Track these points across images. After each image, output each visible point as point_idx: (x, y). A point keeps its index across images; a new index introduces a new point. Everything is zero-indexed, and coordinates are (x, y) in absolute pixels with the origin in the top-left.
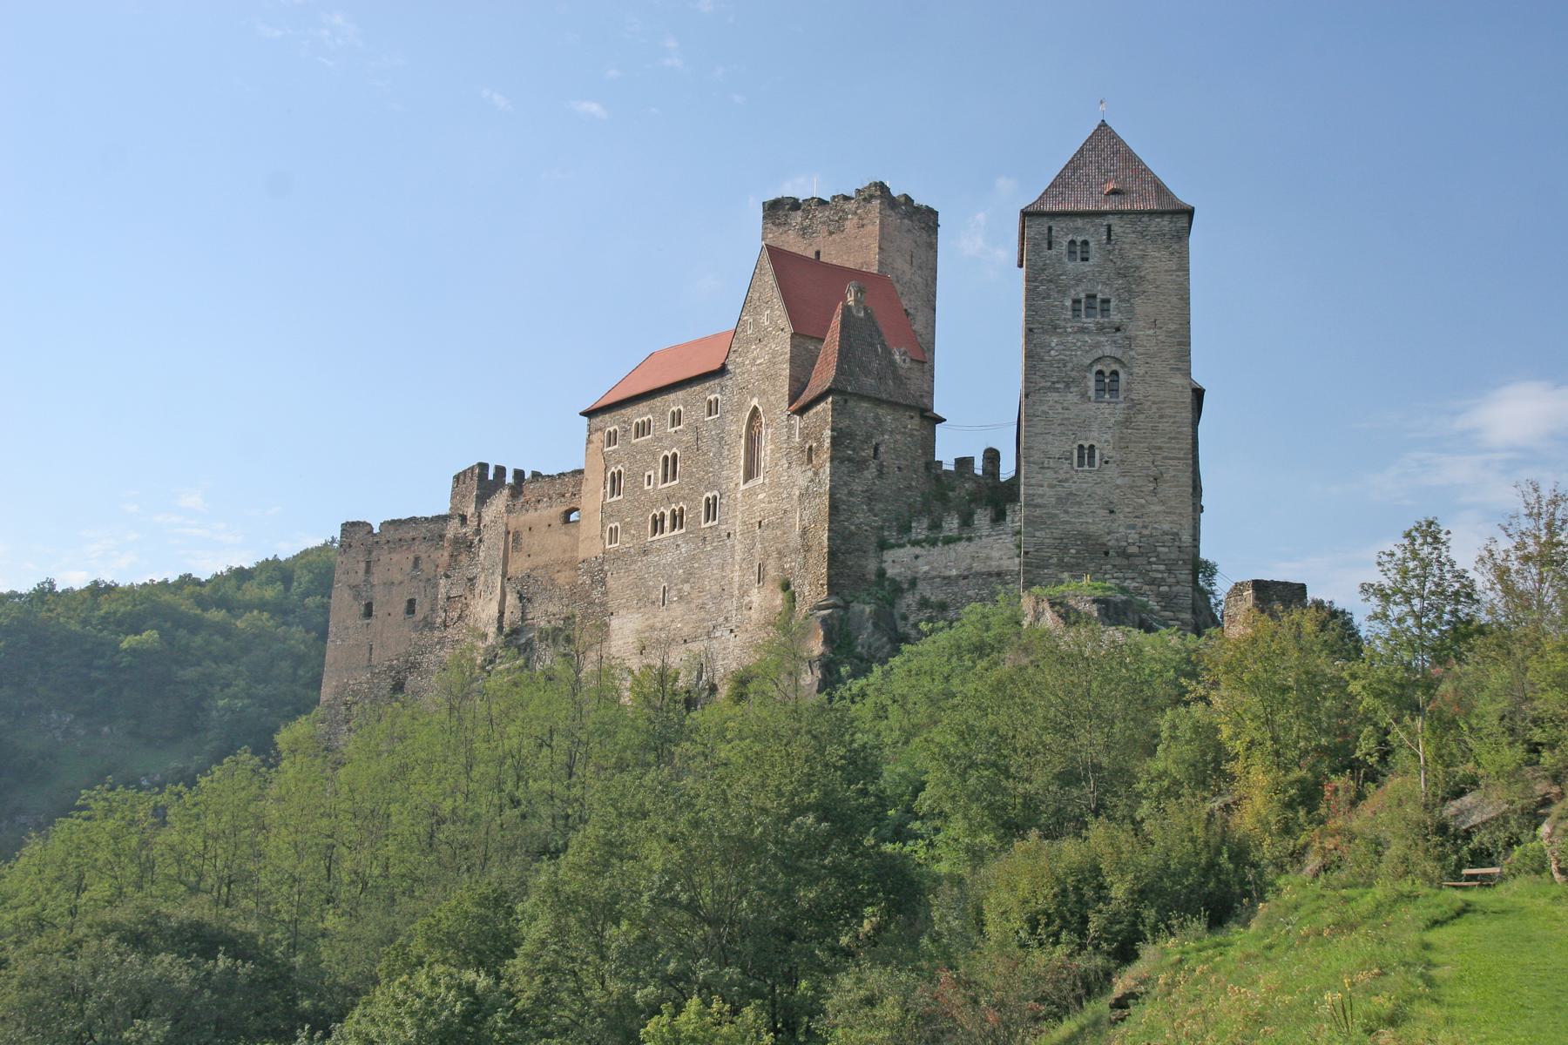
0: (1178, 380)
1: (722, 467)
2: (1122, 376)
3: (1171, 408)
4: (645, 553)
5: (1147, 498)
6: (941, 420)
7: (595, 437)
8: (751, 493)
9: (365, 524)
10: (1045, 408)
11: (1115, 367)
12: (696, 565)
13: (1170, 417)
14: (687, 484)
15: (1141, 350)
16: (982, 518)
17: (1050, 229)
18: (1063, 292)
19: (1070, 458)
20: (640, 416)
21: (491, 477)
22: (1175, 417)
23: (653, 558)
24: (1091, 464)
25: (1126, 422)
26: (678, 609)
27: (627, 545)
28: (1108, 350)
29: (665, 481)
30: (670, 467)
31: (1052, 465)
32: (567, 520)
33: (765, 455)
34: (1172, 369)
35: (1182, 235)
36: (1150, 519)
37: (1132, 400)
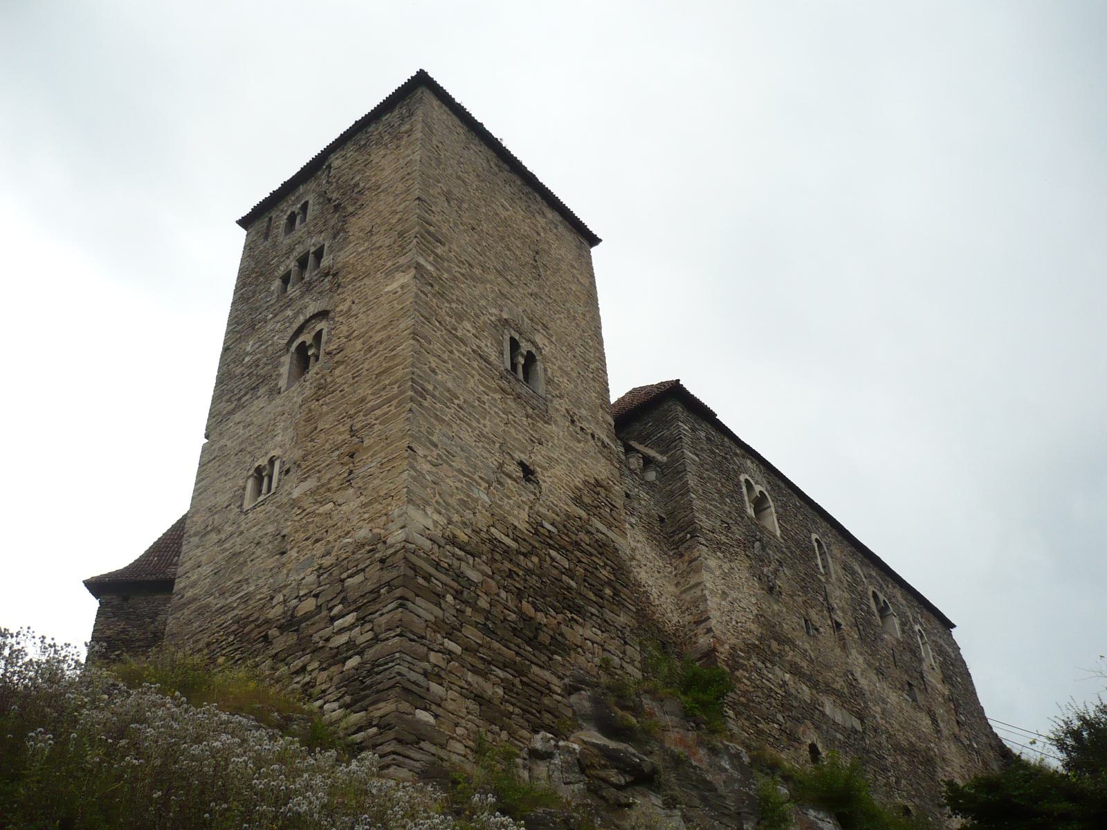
28: (312, 309)
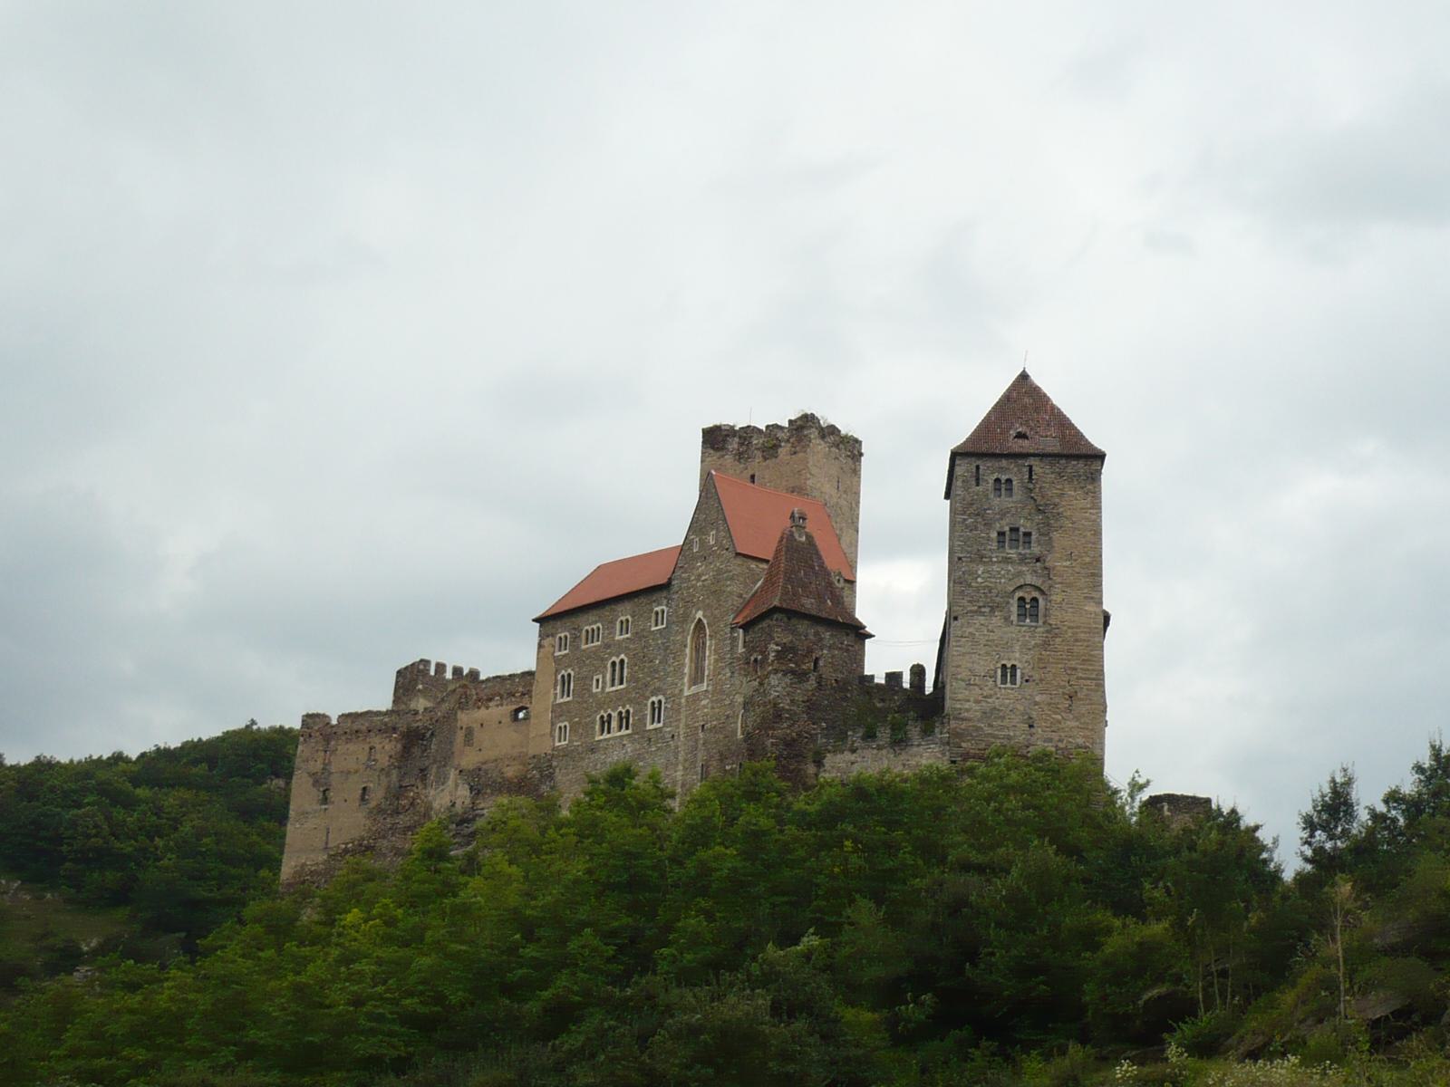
0: (1090, 607)
1: (667, 675)
2: (1041, 601)
3: (1085, 633)
4: (593, 751)
5: (1063, 714)
6: (870, 636)
7: (546, 643)
8: (695, 698)
9: (324, 716)
10: (971, 630)
11: (1036, 594)
12: (641, 764)
13: (1084, 640)
14: (634, 688)
15: (1059, 580)
16: (914, 731)
17: (978, 467)
18: (988, 525)
19: (994, 676)
20: (590, 624)
21: (432, 673)
22: (1089, 641)
23: (596, 756)
24: (1013, 682)
25: (1046, 645)
27: (575, 744)
28: (1029, 579)
29: (613, 685)
31: (977, 682)
32: (516, 719)
33: (709, 664)
34: (1085, 598)
35: (1095, 477)
36: (1066, 734)
37: (1051, 625)
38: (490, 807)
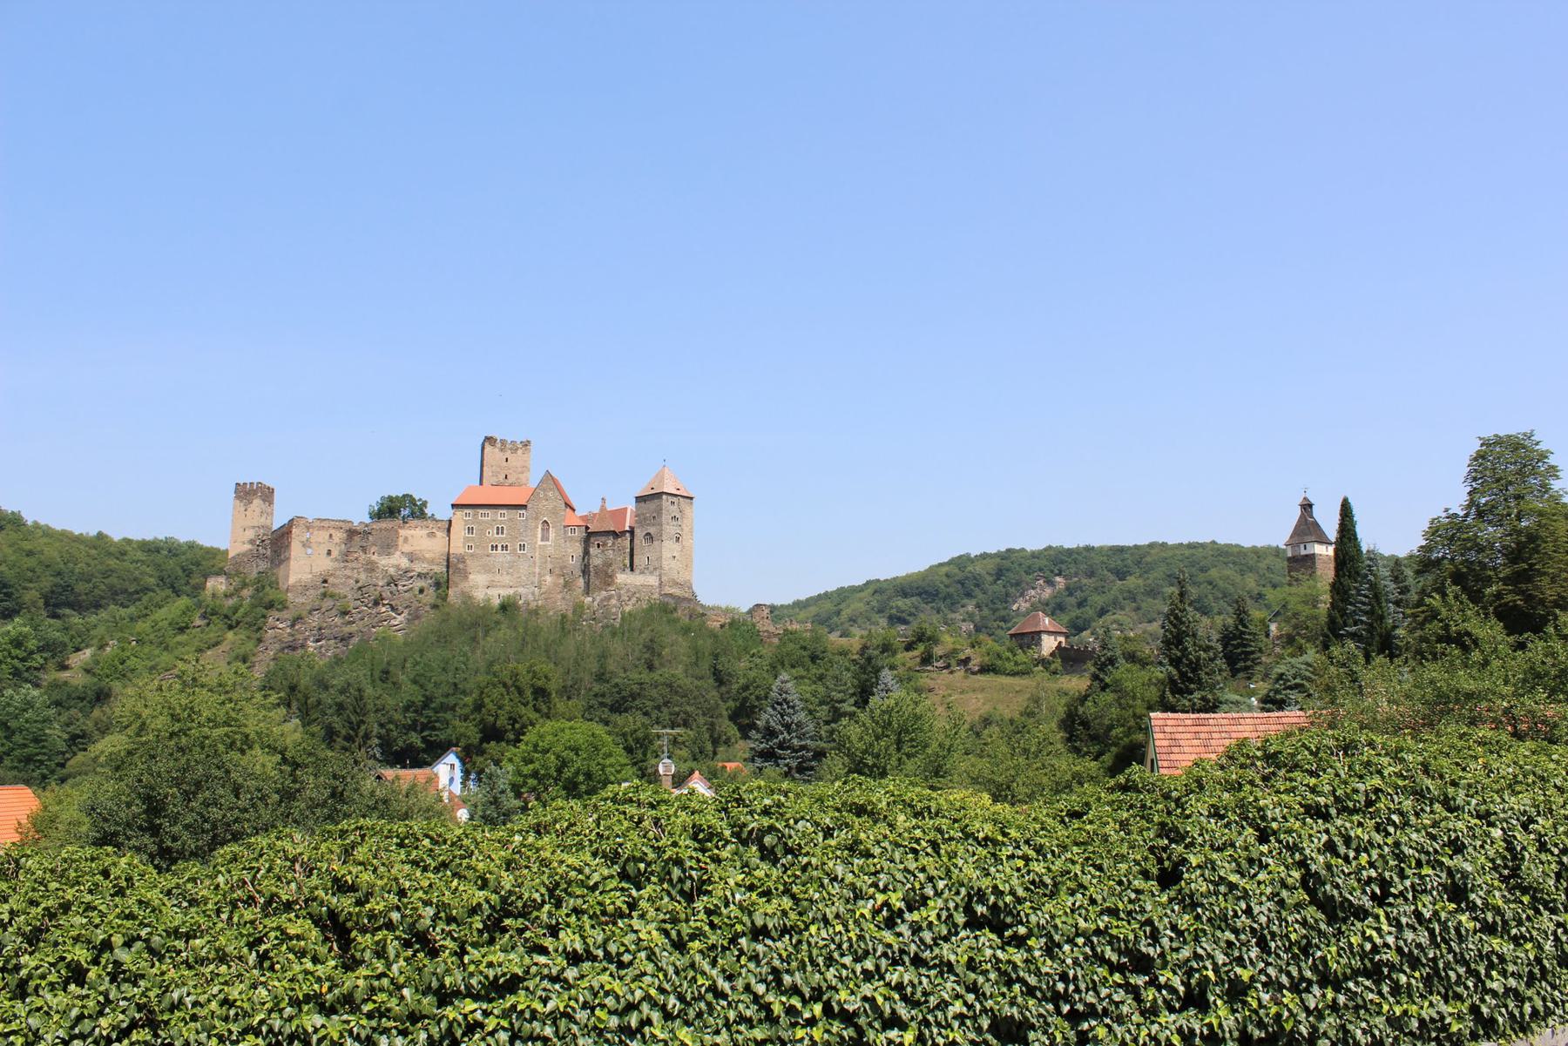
26: (508, 577)
30: (500, 531)
38: (419, 567)
